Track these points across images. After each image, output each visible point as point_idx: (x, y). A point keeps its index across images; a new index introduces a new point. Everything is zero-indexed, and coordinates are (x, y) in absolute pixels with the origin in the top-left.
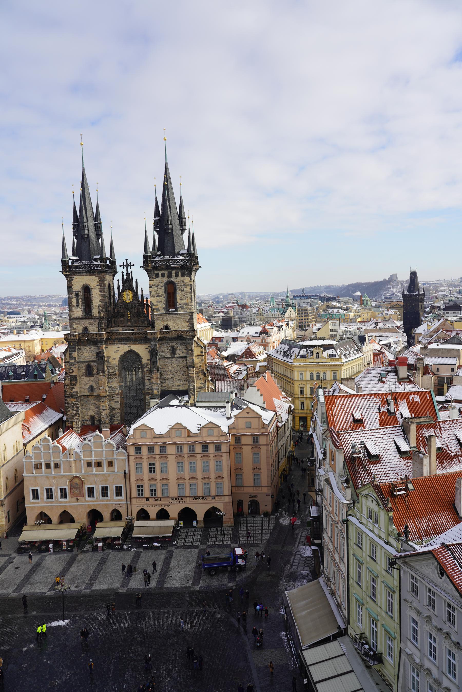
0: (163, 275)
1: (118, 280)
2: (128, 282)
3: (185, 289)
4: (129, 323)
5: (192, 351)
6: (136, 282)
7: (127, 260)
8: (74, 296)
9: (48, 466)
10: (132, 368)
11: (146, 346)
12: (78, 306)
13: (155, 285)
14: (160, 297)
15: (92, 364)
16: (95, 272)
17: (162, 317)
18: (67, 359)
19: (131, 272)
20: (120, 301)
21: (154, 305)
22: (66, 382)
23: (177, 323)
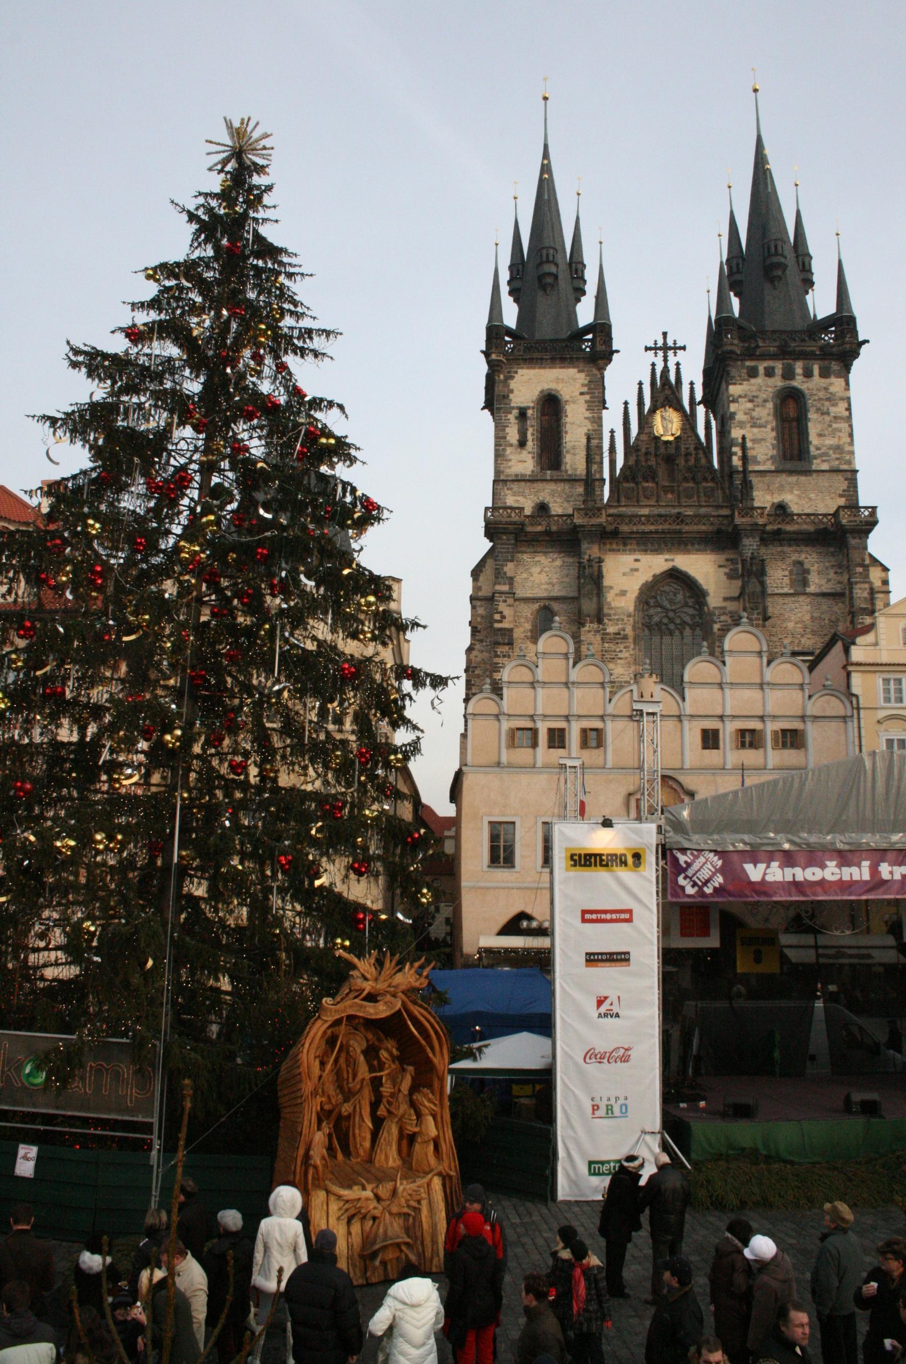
0: (769, 373)
1: (640, 384)
3: (833, 410)
4: (670, 496)
5: (866, 567)
7: (665, 334)
9: (557, 739)
10: (672, 626)
11: (721, 558)
12: (522, 444)
13: (745, 396)
14: (760, 426)
15: (556, 606)
17: (767, 479)
19: (678, 364)
22: (472, 657)
23: (810, 499)
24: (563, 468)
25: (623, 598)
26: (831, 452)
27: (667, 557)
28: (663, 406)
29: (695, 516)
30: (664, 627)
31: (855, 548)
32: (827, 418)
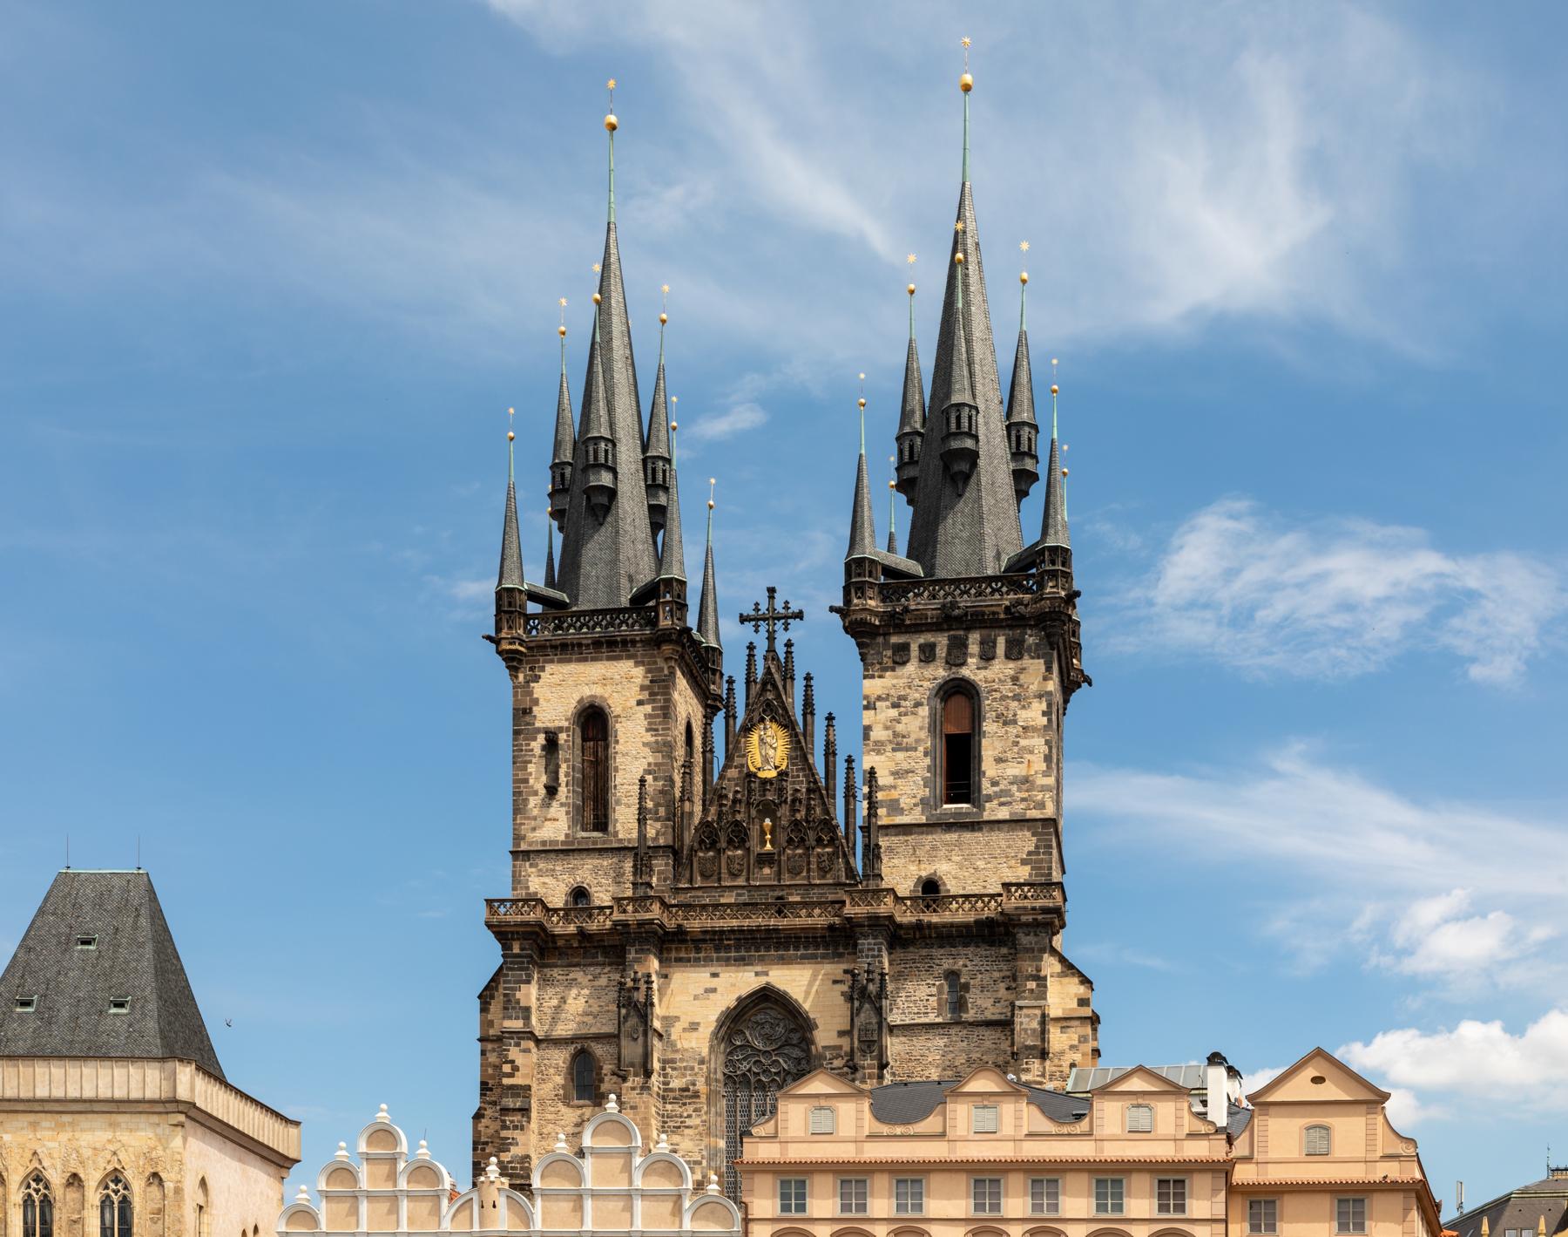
0: (928, 654)
2: (773, 693)
4: (767, 871)
5: (1041, 980)
6: (808, 687)
7: (772, 591)
8: (538, 751)
11: (836, 969)
12: (552, 791)
14: (907, 750)
15: (599, 1050)
16: (634, 642)
18: (491, 1024)
20: (732, 773)
21: (882, 789)
22: (481, 1127)
24: (611, 828)
25: (695, 1034)
26: (1014, 788)
27: (759, 968)
28: (762, 720)
29: (804, 904)
30: (753, 1080)
31: (1027, 950)
32: (1012, 730)
